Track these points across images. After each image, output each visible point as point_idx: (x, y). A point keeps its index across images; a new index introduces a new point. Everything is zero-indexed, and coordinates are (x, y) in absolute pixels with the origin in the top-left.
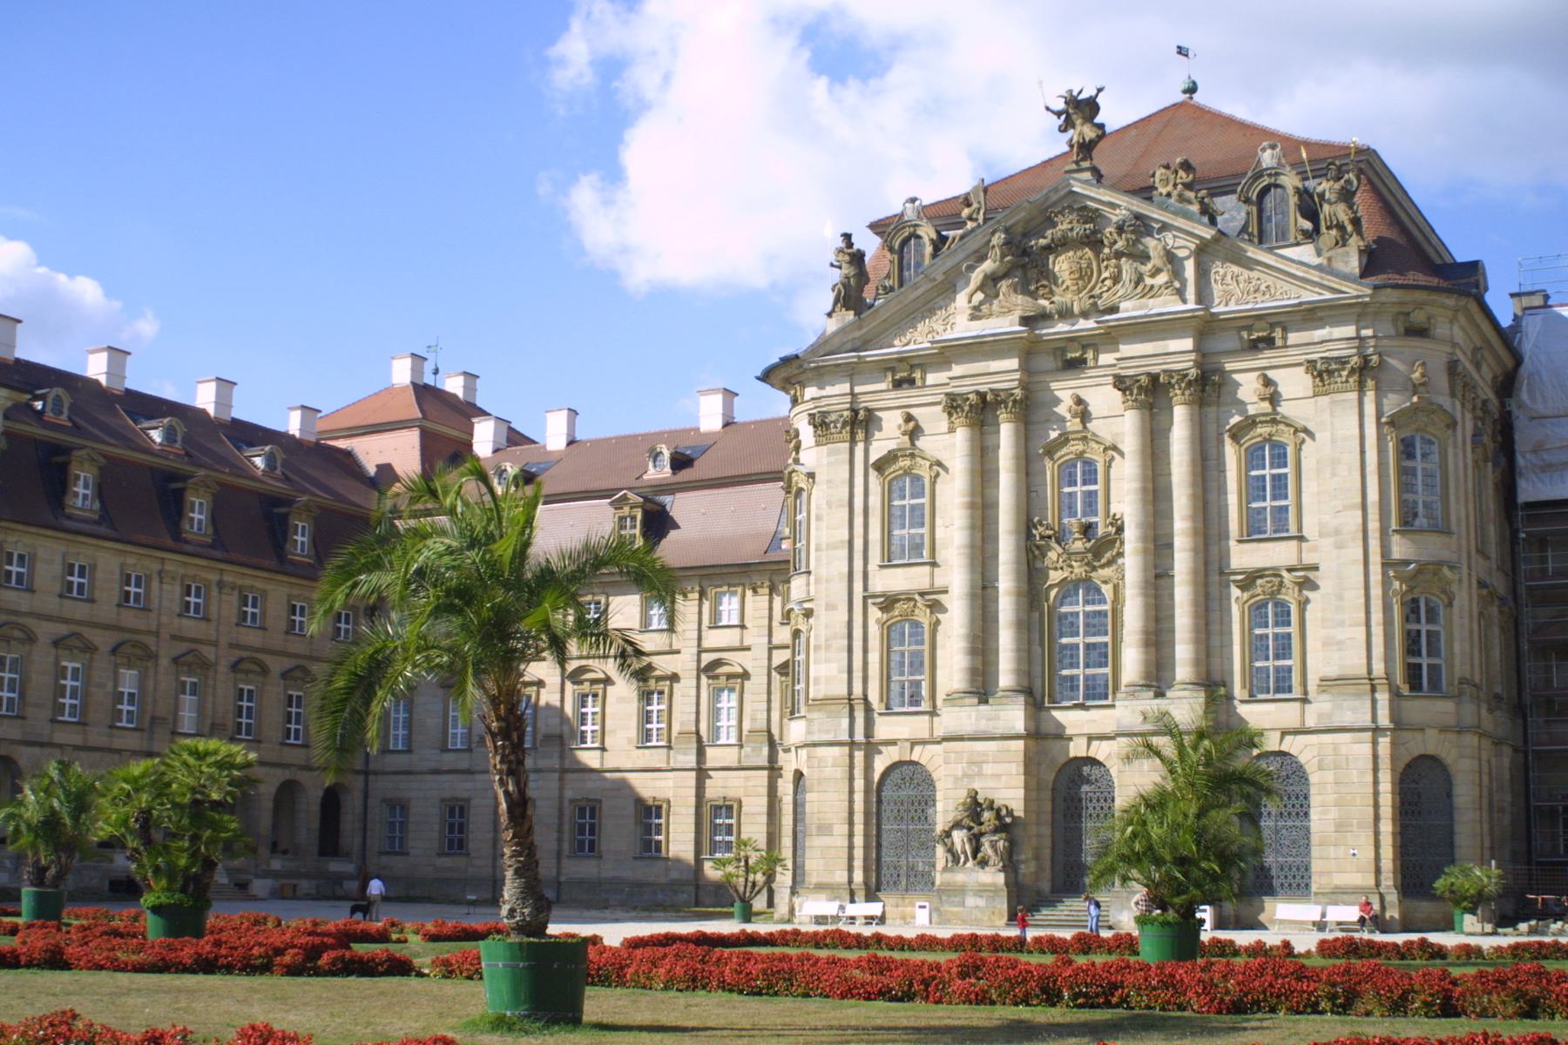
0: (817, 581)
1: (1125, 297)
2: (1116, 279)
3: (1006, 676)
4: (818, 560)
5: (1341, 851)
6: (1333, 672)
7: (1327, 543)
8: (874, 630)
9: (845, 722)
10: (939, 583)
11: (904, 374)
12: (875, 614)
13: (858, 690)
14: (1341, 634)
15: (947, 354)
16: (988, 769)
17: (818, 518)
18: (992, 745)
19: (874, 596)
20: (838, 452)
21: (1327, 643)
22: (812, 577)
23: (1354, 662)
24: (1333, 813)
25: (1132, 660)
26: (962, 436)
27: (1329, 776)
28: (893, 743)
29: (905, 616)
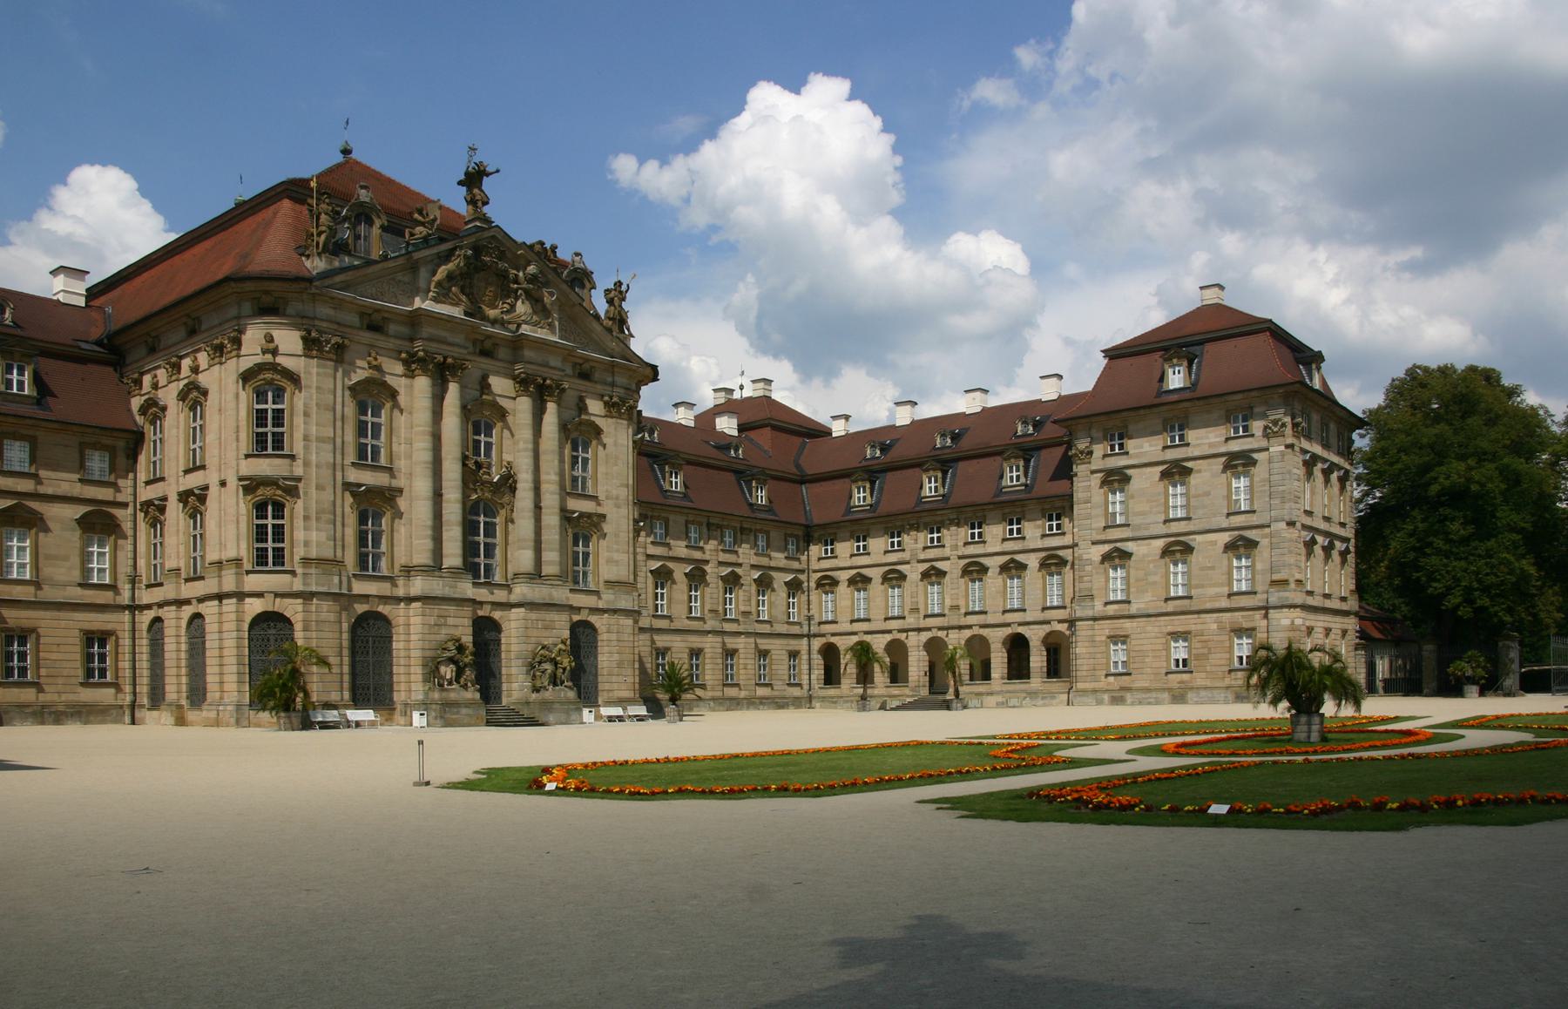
0: (306, 464)
1: (526, 323)
2: (513, 307)
3: (453, 555)
4: (306, 448)
5: (621, 679)
6: (613, 578)
7: (610, 502)
8: (348, 509)
9: (336, 579)
10: (395, 483)
11: (375, 324)
12: (349, 499)
13: (339, 553)
14: (616, 556)
15: (416, 318)
16: (451, 621)
17: (306, 414)
18: (452, 609)
19: (350, 484)
20: (325, 367)
21: (609, 561)
22: (300, 462)
23: (622, 572)
24: (616, 657)
25: (523, 558)
26: (423, 384)
27: (614, 637)
28: (367, 596)
29: (374, 505)
